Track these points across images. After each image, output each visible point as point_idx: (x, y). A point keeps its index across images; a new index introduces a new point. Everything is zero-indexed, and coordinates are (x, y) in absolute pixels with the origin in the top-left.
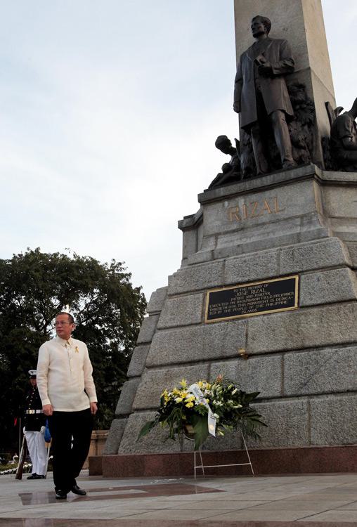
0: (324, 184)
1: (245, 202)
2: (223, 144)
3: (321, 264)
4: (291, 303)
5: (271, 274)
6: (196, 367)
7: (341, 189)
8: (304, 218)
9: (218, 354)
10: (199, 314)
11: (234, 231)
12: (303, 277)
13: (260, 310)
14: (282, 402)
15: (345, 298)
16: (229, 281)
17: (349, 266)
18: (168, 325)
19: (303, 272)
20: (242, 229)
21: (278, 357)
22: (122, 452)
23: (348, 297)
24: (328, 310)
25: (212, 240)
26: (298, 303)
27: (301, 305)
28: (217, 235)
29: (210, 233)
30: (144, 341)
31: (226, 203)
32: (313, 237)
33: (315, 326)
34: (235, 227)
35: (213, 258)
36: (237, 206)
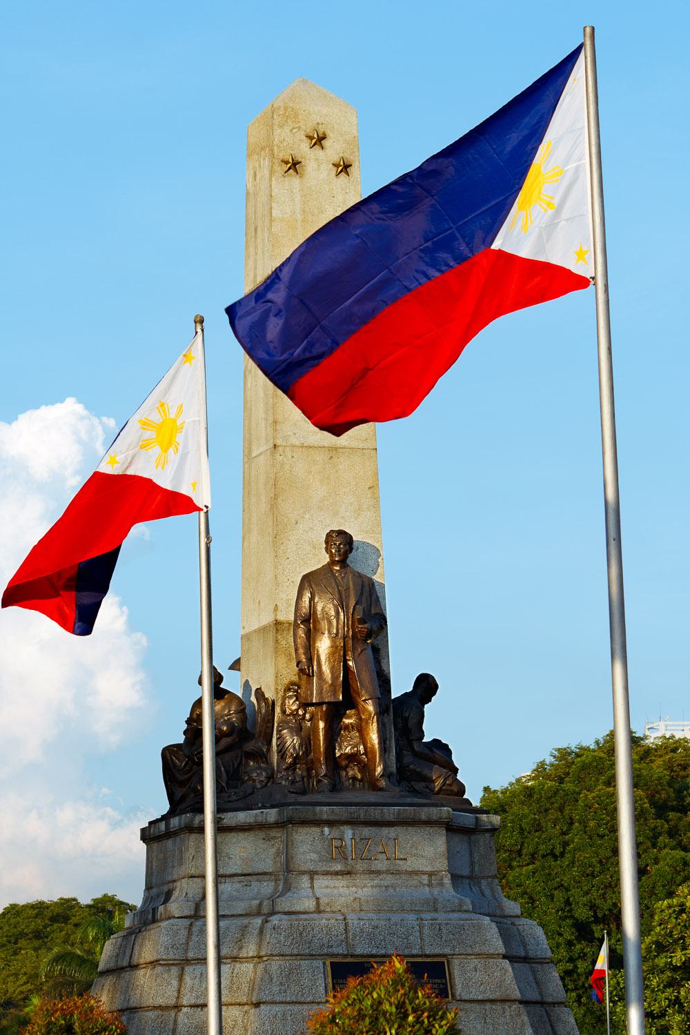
1: (354, 834)
5: (415, 952)
8: (433, 877)
10: (322, 989)
11: (337, 873)
15: (510, 998)
16: (359, 951)
17: (505, 957)
18: (278, 999)
19: (454, 955)
20: (349, 873)
23: (513, 997)
24: (491, 1008)
25: (305, 880)
26: (452, 995)
27: (458, 998)
28: (312, 874)
30: (164, 1005)
32: (454, 908)
33: (479, 1026)
34: (338, 867)
35: (318, 911)
36: (341, 839)
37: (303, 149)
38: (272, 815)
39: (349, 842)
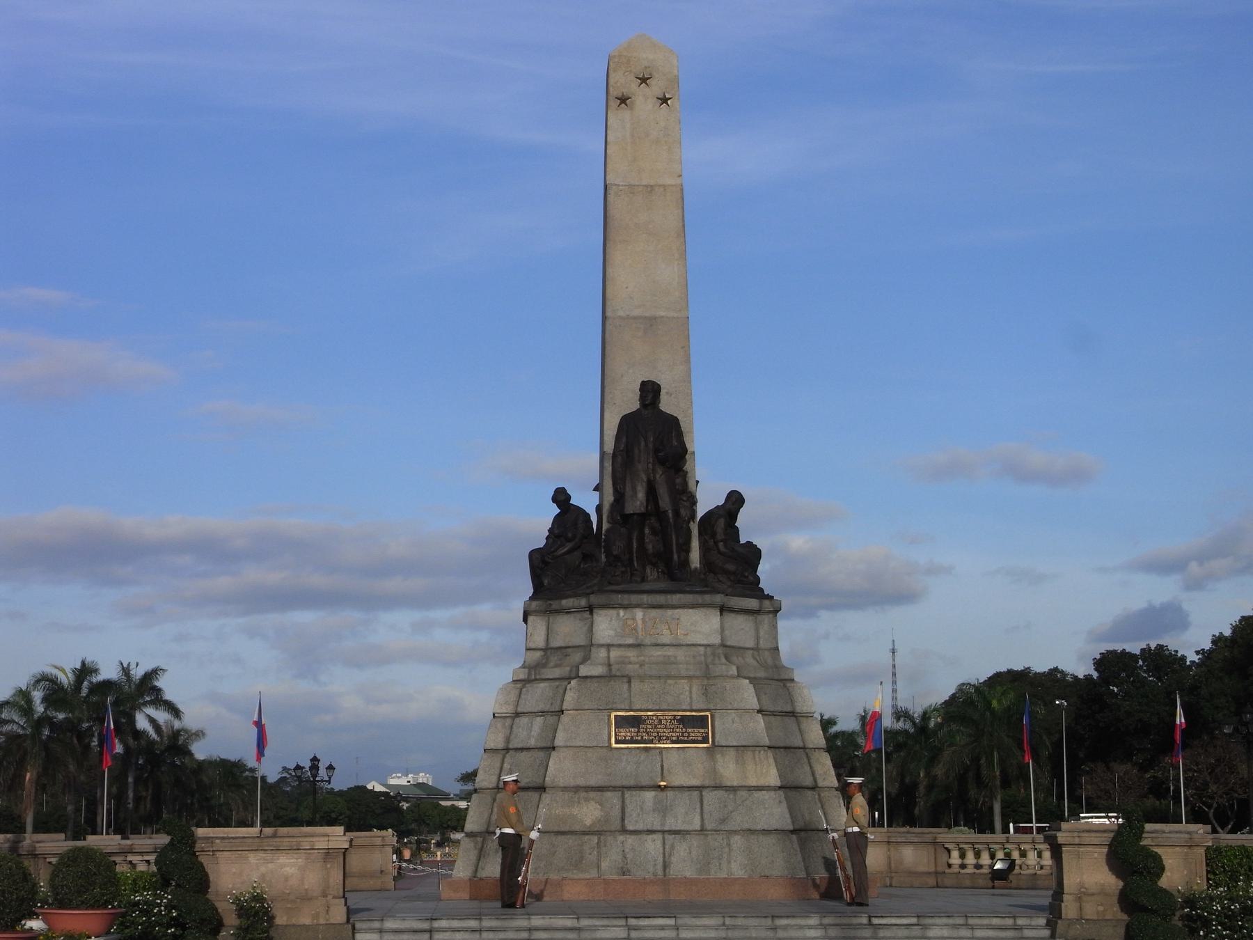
0: (723, 609)
2: (561, 497)
3: (735, 706)
4: (705, 740)
7: (733, 615)
9: (632, 783)
10: (606, 738)
11: (630, 646)
12: (717, 715)
13: (673, 742)
17: (759, 711)
21: (696, 794)
29: (602, 642)
31: (622, 612)
34: (630, 641)
37: (633, 87)
38: (583, 602)
39: (640, 622)
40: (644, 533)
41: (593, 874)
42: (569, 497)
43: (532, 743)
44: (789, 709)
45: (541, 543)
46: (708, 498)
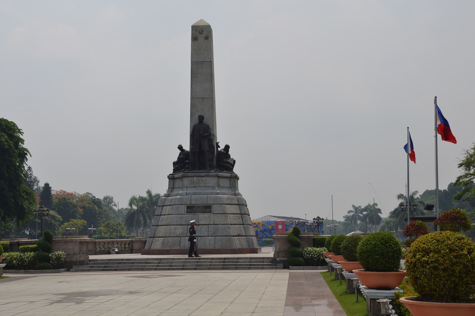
0: (219, 177)
2: (180, 148)
4: (210, 212)
6: (183, 226)
14: (208, 237)
22: (152, 248)
28: (187, 187)
40: (204, 157)
41: (179, 248)
42: (182, 147)
43: (167, 213)
44: (237, 203)
45: (175, 159)
46: (222, 147)
